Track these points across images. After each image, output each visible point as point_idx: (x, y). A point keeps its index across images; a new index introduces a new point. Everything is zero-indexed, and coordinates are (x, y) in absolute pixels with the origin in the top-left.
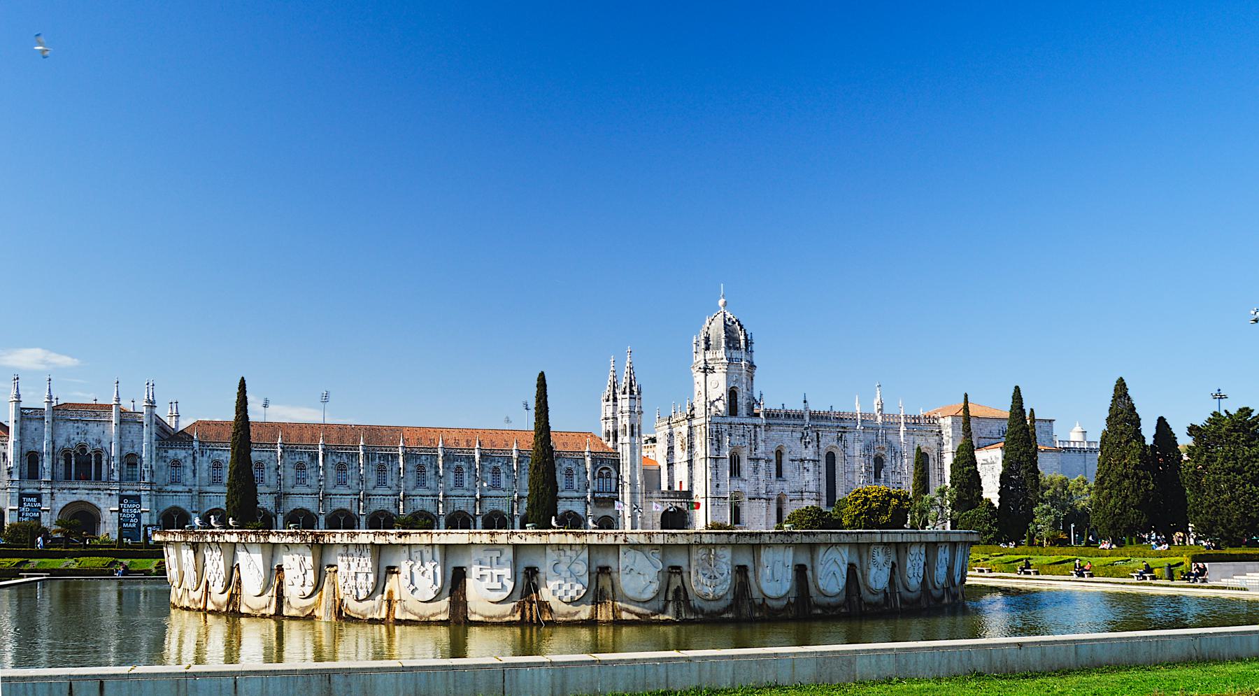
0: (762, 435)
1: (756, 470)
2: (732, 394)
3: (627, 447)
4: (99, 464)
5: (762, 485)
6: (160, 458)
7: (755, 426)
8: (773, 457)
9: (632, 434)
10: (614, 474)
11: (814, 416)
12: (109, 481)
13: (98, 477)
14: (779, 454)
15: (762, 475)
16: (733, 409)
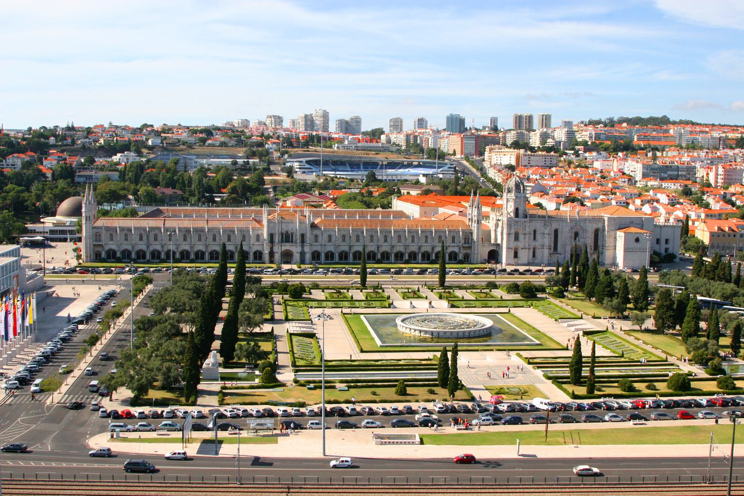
0: (527, 225)
1: (525, 238)
2: (517, 210)
3: (476, 228)
4: (292, 237)
5: (527, 244)
6: (312, 234)
7: (525, 222)
8: (532, 233)
9: (478, 223)
10: (470, 237)
11: (550, 217)
12: (296, 242)
13: (292, 242)
14: (535, 231)
15: (527, 240)
16: (517, 215)
